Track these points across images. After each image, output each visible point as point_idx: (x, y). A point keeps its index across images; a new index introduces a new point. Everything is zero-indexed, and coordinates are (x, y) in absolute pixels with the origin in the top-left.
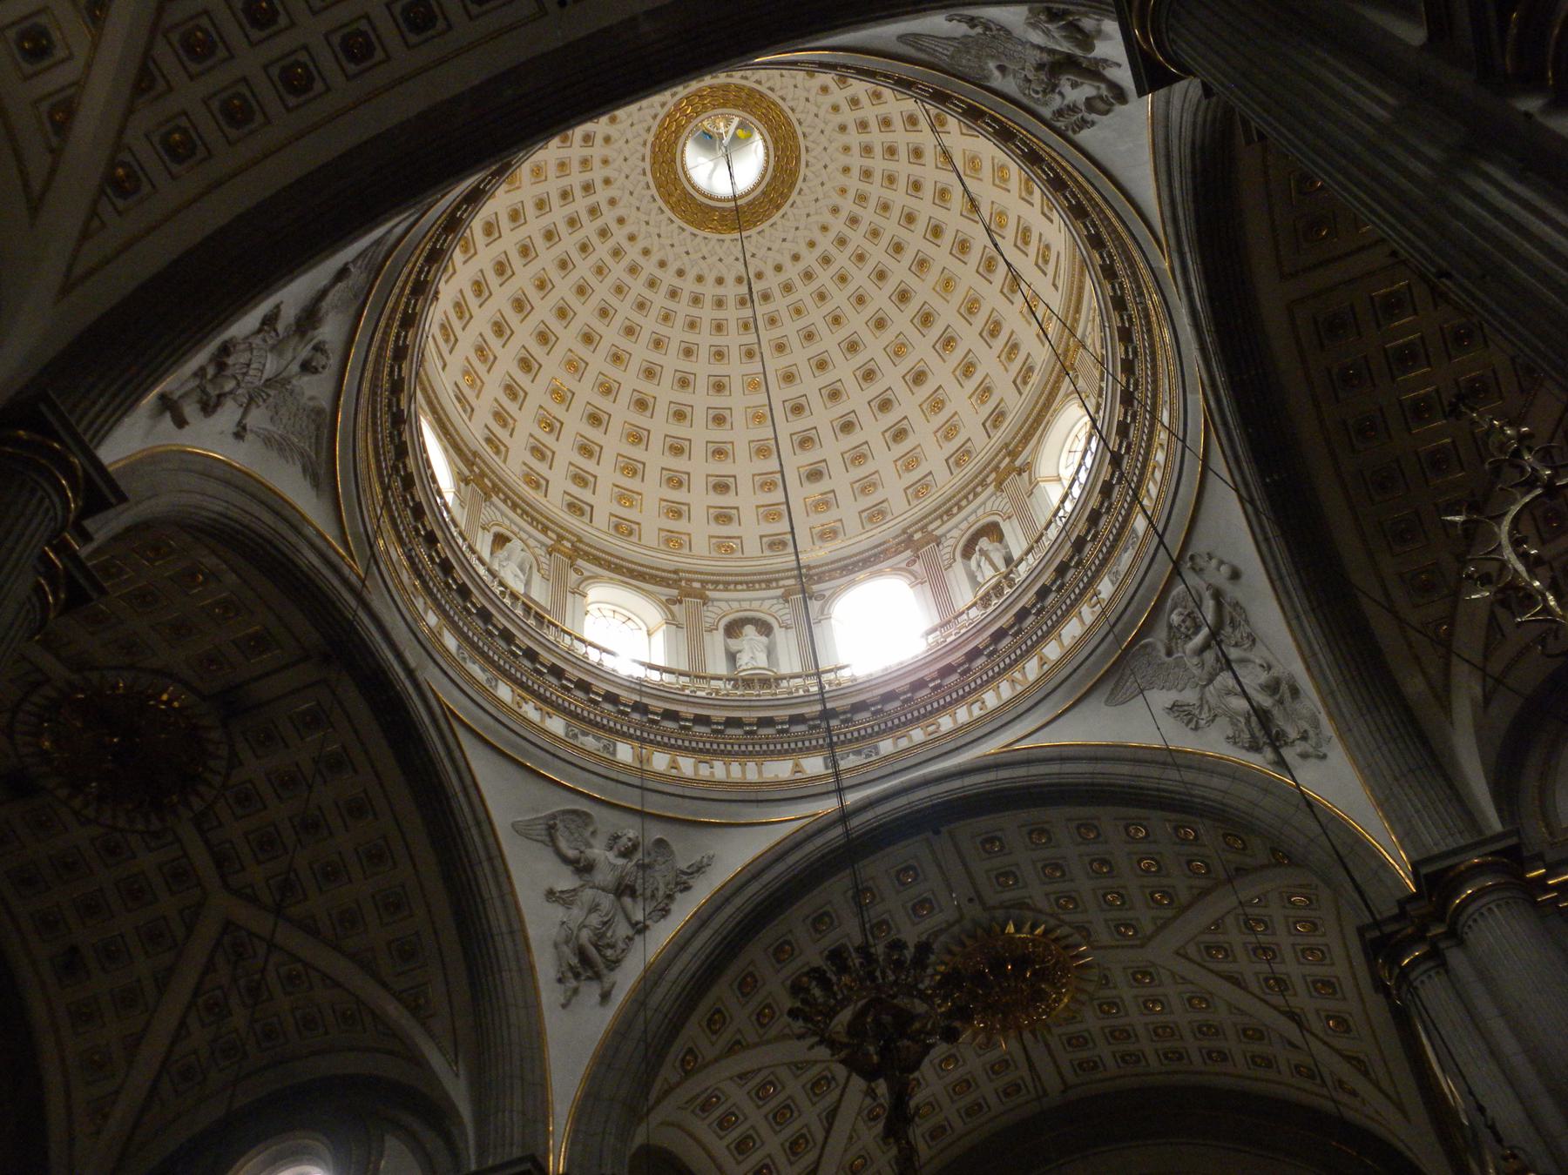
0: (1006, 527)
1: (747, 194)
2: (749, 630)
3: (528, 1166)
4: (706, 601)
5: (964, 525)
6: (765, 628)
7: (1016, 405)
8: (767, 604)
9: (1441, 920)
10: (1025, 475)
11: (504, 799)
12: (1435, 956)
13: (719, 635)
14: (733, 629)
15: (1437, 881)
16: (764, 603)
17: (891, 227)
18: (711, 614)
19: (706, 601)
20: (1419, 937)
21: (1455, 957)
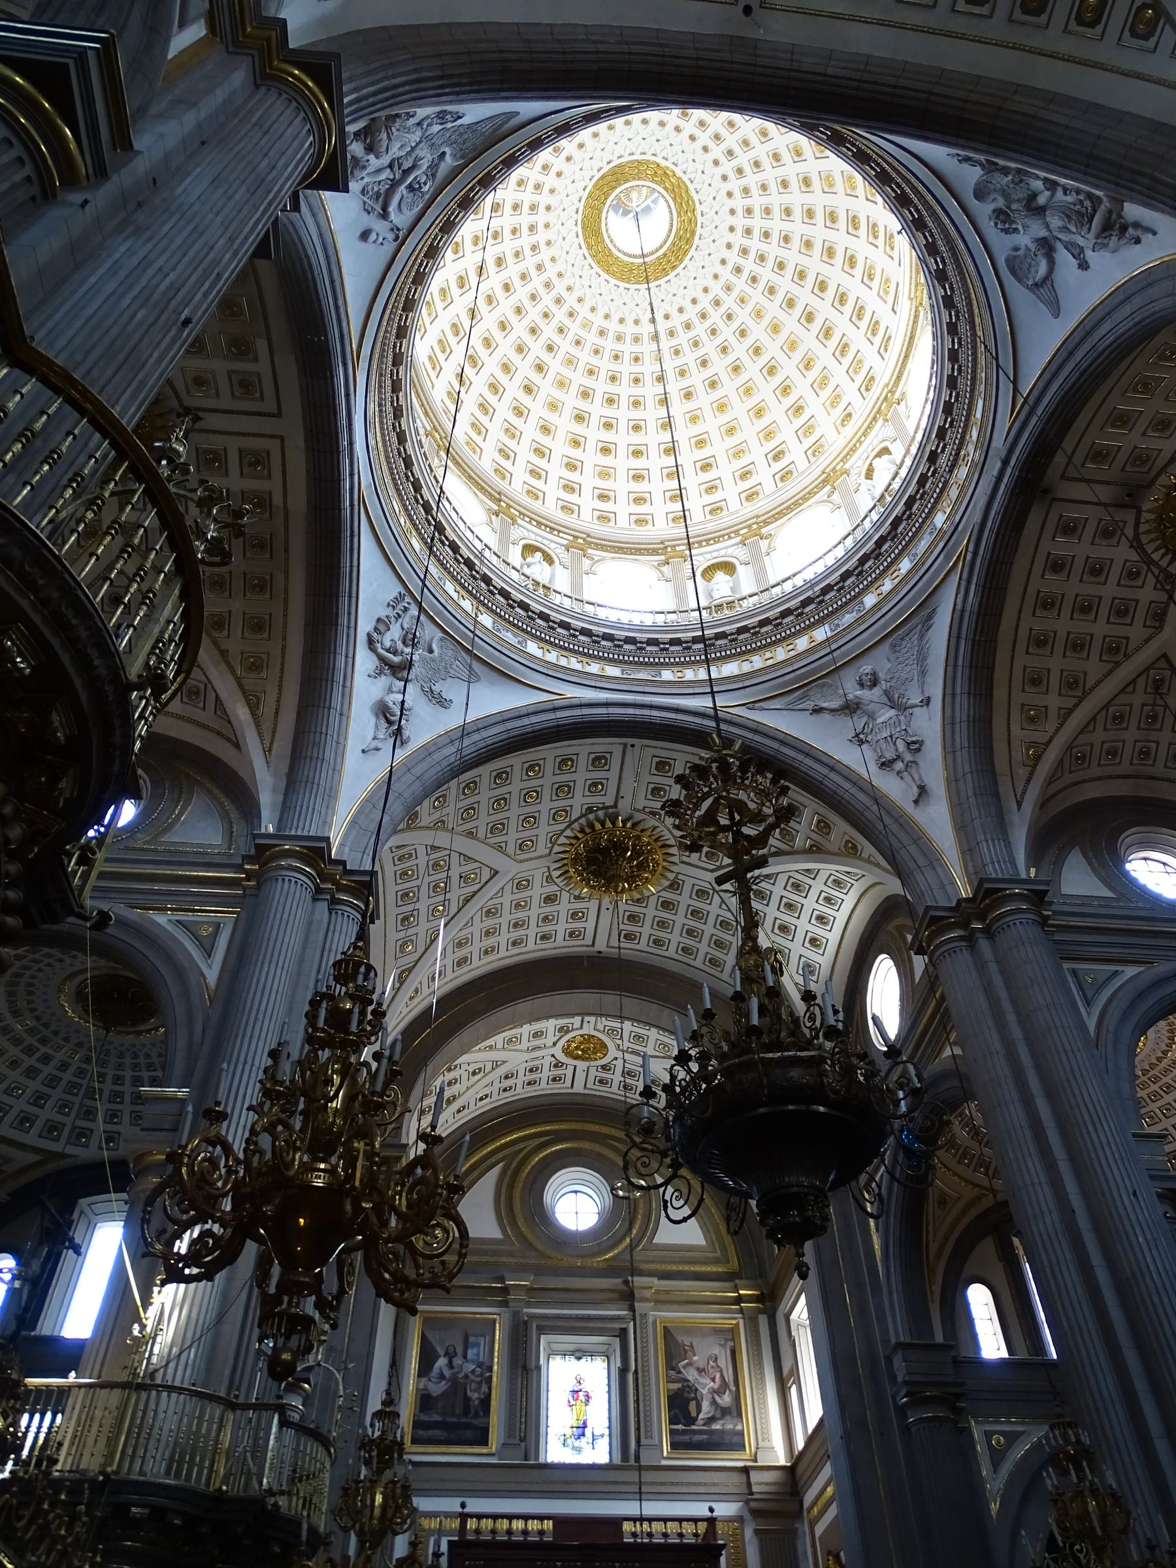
0: (740, 569)
1: (652, 253)
2: (538, 554)
3: (324, 845)
4: (514, 522)
5: (708, 556)
6: (548, 559)
7: (771, 495)
8: (553, 545)
9: (981, 918)
10: (766, 542)
11: (373, 588)
12: (970, 939)
13: (519, 549)
14: (529, 549)
15: (988, 895)
16: (554, 544)
17: (727, 333)
18: (516, 533)
19: (514, 522)
20: (965, 925)
21: (984, 944)
